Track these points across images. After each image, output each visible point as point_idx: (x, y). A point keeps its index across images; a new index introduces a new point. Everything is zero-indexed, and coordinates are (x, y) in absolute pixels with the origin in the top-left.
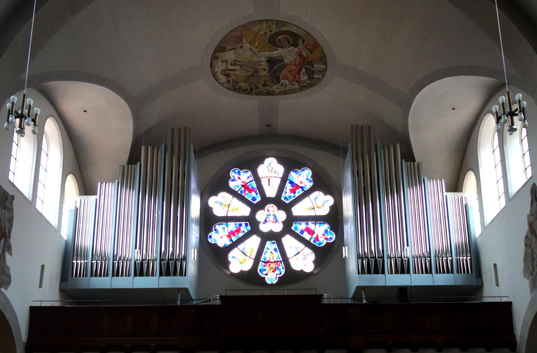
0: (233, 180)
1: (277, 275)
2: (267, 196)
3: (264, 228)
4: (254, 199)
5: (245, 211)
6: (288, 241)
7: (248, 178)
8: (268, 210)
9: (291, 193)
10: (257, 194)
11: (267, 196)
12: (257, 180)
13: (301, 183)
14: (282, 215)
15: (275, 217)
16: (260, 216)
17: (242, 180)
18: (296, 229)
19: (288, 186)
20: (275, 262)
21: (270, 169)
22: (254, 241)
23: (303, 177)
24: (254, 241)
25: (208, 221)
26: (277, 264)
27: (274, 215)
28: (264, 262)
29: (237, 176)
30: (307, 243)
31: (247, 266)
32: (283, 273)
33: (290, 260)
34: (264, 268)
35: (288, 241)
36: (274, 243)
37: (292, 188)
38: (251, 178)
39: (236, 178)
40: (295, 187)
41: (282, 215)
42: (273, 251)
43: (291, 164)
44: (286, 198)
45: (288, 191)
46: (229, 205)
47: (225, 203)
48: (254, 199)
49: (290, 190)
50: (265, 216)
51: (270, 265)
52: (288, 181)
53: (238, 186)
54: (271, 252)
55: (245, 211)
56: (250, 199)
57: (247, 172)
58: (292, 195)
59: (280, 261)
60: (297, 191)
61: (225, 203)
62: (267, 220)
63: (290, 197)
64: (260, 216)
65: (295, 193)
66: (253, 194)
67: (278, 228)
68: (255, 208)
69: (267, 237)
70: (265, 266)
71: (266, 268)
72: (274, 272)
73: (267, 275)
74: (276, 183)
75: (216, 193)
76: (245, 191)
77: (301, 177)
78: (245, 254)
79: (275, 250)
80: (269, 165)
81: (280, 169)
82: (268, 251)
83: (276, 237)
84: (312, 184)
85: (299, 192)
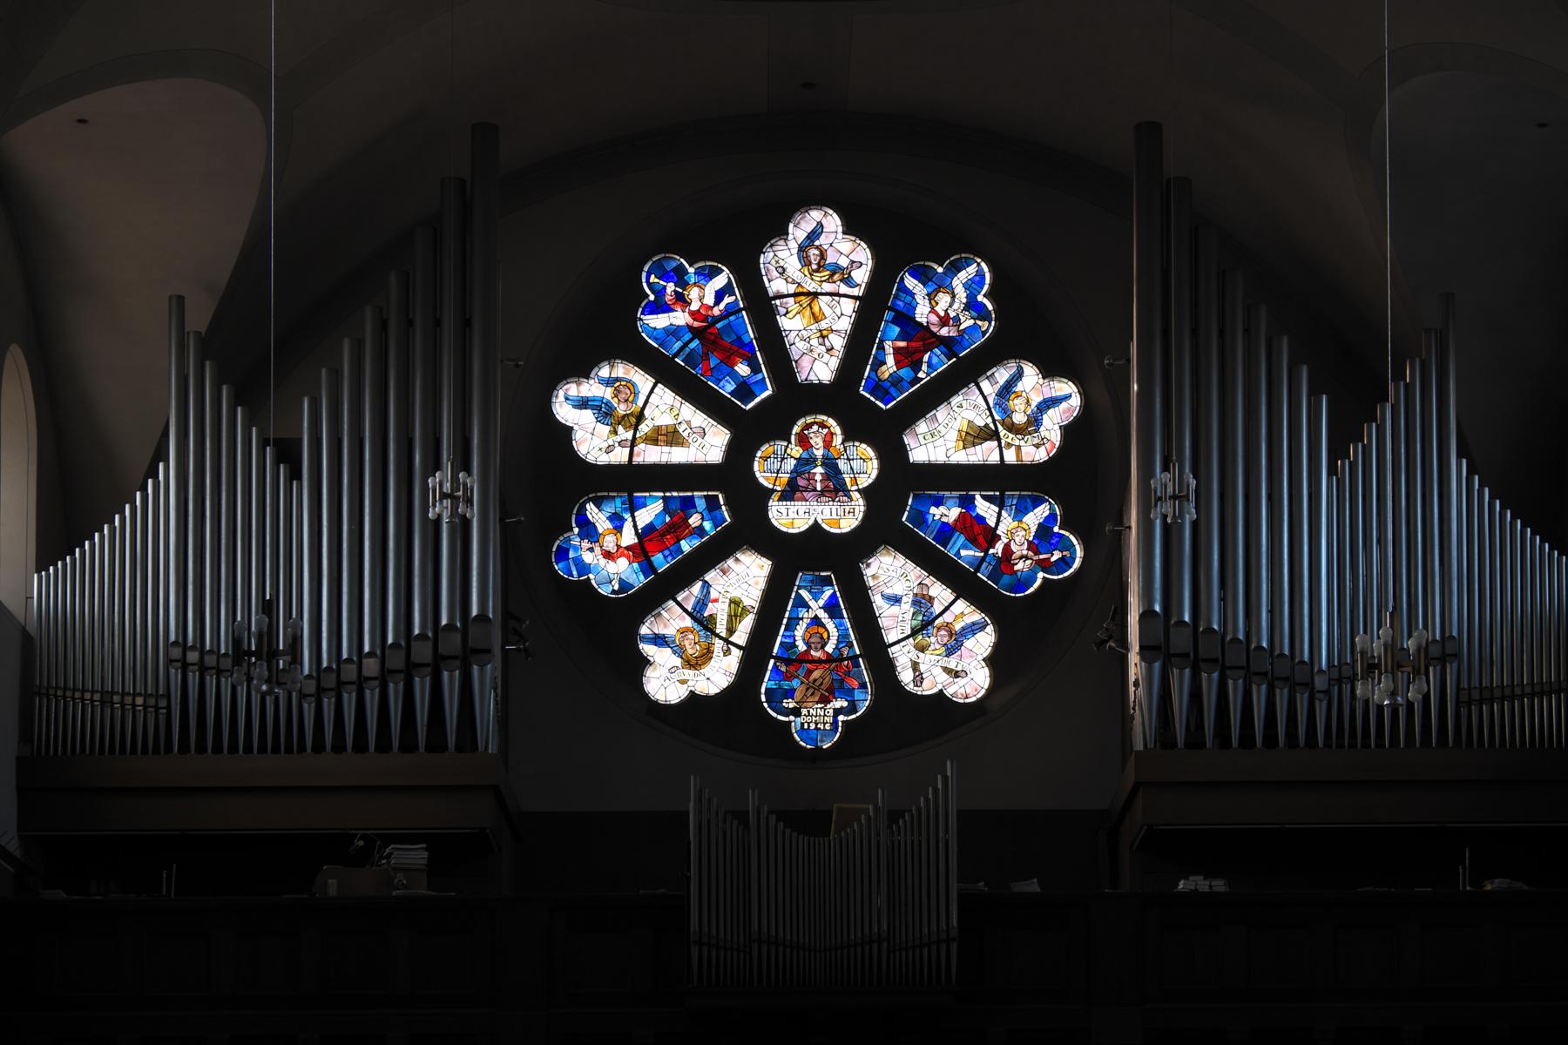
0: (659, 307)
1: (837, 712)
2: (801, 377)
3: (789, 517)
4: (745, 390)
5: (709, 443)
6: (890, 573)
7: (719, 296)
8: (804, 441)
9: (899, 364)
10: (755, 369)
11: (801, 377)
12: (762, 307)
13: (944, 321)
14: (863, 465)
15: (832, 471)
16: (770, 467)
17: (695, 306)
18: (920, 518)
19: (890, 341)
20: (830, 659)
21: (813, 252)
22: (744, 577)
23: (950, 300)
24: (744, 577)
25: (557, 486)
26: (836, 669)
27: (830, 464)
28: (788, 662)
29: (671, 287)
30: (963, 583)
31: (718, 675)
32: (862, 709)
33: (891, 650)
34: (786, 685)
35: (890, 573)
36: (827, 582)
37: (902, 344)
38: (735, 298)
39: (669, 298)
40: (918, 338)
41: (863, 465)
42: (822, 615)
43: (904, 242)
44: (878, 388)
45: (890, 360)
46: (640, 417)
47: (621, 409)
48: (745, 390)
49: (897, 351)
50: (790, 464)
51: (810, 672)
52: (888, 315)
53: (673, 332)
54: (816, 621)
55: (709, 443)
56: (727, 388)
57: (715, 272)
58: (905, 373)
59: (856, 657)
60: (926, 358)
61: (621, 409)
62: (802, 482)
63: (896, 381)
64: (770, 467)
65: (916, 367)
66: (743, 369)
67: (844, 517)
68: (749, 433)
69: (797, 557)
70: (789, 677)
71: (795, 683)
72: (825, 700)
73: (796, 712)
74: (841, 315)
75: (584, 373)
76: (705, 357)
77: (943, 300)
78: (706, 628)
79: (831, 608)
80: (814, 235)
81: (856, 256)
82: (802, 613)
83: (834, 558)
84: (988, 327)
85: (934, 364)
